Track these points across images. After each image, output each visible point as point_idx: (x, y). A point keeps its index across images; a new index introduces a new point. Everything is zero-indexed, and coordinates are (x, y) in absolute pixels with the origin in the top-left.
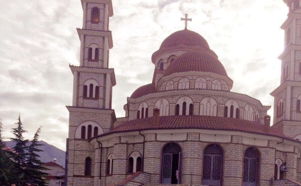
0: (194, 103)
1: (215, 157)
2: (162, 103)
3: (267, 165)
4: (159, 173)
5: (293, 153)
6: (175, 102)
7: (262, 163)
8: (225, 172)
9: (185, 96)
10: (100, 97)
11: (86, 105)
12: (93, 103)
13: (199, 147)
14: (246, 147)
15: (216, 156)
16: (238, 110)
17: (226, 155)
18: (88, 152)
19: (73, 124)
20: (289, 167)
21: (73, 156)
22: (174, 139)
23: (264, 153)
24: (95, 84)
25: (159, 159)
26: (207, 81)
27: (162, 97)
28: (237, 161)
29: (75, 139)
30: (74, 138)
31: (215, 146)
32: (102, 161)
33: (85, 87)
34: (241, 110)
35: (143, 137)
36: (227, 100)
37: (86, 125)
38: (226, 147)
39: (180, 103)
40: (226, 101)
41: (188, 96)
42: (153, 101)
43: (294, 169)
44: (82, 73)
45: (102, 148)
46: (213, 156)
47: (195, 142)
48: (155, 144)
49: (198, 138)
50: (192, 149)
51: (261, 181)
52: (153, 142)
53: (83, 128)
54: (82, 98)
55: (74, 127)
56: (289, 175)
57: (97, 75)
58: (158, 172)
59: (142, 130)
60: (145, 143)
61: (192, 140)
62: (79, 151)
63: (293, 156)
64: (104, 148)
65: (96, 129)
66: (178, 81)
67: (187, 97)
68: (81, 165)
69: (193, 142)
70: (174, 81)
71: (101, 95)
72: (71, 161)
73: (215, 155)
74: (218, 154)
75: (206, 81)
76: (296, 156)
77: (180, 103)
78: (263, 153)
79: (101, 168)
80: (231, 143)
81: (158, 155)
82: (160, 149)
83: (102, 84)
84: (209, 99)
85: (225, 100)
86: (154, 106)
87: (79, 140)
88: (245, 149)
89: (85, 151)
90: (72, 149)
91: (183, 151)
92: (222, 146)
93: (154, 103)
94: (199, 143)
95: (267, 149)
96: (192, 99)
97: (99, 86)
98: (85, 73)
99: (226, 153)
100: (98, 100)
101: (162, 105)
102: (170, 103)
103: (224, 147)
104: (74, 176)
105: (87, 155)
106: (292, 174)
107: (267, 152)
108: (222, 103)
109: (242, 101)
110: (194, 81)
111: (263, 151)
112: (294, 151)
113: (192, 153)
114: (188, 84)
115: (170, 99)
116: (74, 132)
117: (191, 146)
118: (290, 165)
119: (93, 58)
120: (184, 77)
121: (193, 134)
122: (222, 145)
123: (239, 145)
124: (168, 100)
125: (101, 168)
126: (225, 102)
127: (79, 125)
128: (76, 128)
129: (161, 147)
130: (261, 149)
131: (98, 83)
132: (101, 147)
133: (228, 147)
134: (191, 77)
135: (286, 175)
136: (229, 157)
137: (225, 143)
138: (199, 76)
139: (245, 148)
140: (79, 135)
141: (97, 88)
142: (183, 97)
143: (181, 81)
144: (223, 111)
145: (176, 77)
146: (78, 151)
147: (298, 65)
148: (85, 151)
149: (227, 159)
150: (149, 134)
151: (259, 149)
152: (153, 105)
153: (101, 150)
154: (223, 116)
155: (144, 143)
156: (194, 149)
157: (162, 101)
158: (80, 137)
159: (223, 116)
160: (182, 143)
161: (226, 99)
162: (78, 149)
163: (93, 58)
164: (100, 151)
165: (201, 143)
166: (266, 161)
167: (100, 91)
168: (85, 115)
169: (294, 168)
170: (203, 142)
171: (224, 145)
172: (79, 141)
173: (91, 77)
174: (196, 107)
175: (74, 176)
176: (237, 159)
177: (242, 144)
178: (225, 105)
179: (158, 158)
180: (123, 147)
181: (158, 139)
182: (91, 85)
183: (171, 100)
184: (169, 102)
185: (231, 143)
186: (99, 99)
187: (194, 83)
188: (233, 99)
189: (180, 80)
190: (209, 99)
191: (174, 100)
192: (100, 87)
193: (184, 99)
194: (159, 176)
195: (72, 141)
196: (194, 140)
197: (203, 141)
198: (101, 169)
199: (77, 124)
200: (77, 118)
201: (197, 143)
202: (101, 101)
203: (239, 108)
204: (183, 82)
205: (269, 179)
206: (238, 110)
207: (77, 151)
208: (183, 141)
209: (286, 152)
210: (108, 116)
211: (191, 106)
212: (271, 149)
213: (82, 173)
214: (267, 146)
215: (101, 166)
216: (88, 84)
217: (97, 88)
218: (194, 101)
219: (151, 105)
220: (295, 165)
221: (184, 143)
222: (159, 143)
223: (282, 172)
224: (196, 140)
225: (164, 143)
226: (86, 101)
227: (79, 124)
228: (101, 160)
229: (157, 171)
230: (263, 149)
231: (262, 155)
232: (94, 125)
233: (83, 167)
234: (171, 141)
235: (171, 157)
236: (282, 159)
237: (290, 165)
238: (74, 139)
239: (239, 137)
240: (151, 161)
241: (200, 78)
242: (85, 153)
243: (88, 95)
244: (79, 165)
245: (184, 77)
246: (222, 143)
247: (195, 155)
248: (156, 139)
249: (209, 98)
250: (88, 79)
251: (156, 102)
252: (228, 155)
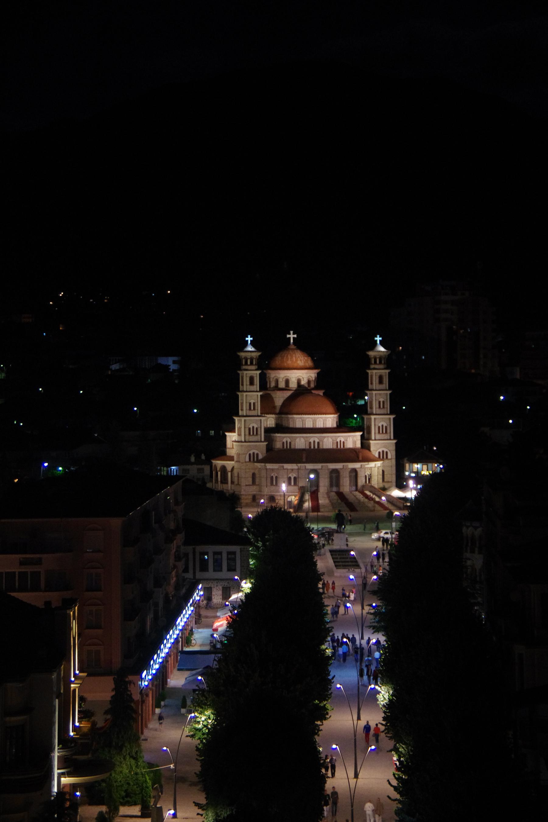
11: (250, 440)
16: (344, 442)
24: (256, 426)
33: (249, 429)
34: (345, 442)
37: (251, 452)
45: (267, 469)
53: (250, 455)
64: (268, 469)
65: (257, 454)
71: (259, 433)
87: (247, 462)
104: (246, 485)
105: (253, 471)
114: (312, 423)
119: (252, 408)
128: (245, 455)
140: (247, 459)
141: (257, 429)
144: (336, 444)
155: (298, 469)
158: (248, 461)
163: (252, 408)
174: (321, 443)
175: (246, 485)
182: (253, 427)
206: (344, 442)
211: (318, 443)
213: (251, 483)
216: (251, 427)
217: (257, 429)
223: (369, 479)
226: (250, 437)
232: (256, 452)
233: (251, 479)
243: (252, 433)
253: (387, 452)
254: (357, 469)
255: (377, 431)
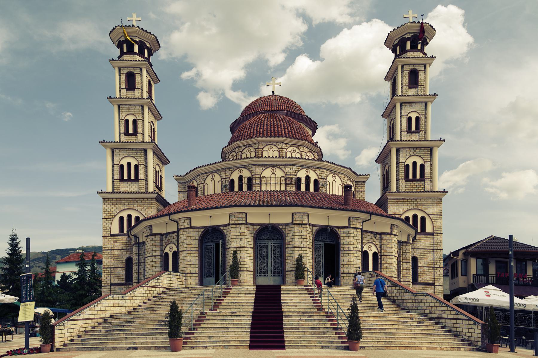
0: (252, 175)
1: (273, 243)
2: (213, 179)
3: (350, 252)
4: (197, 272)
5: (391, 234)
6: (229, 177)
7: (342, 249)
8: (287, 264)
9: (242, 167)
10: (140, 178)
11: (123, 189)
12: (131, 187)
13: (246, 231)
14: (317, 228)
15: (274, 242)
17: (286, 241)
18: (128, 250)
19: (108, 215)
20: (386, 254)
21: (110, 258)
22: (215, 222)
23: (344, 235)
24: (134, 163)
25: (197, 252)
26: (279, 148)
27: (213, 172)
28: (301, 248)
29: (112, 235)
30: (110, 234)
31: (270, 229)
32: (140, 262)
33: (122, 167)
35: (177, 223)
36: (299, 169)
37: (125, 214)
38: (287, 230)
39: (235, 176)
40: (299, 171)
41: (244, 167)
42: (203, 178)
43: (393, 257)
44: (116, 149)
46: (269, 243)
47: (240, 226)
48: (190, 232)
49: (244, 219)
50: (236, 234)
51: (342, 275)
52: (187, 230)
53: (122, 219)
54: (119, 180)
55: (110, 219)
56: (386, 265)
57: (135, 152)
58: (196, 269)
59: (172, 214)
60: (179, 232)
61: (236, 222)
62: (117, 250)
63: (391, 238)
66: (241, 152)
67: (244, 169)
68: (120, 269)
69: (238, 226)
70: (236, 152)
71: (142, 175)
72: (107, 264)
73: (273, 242)
74: (277, 240)
75: (278, 149)
76: (395, 239)
77: (235, 176)
78: (342, 235)
79: (138, 270)
80: (292, 223)
81: (195, 246)
82: (197, 238)
83: (141, 161)
84: (273, 170)
85: (297, 169)
86: (204, 183)
88: (314, 231)
89: (125, 249)
90: (107, 249)
91: (227, 239)
92: (281, 229)
93: (204, 180)
94: (246, 226)
95: (348, 229)
96: (250, 171)
97: (138, 164)
98: (120, 150)
99: (287, 238)
100: (138, 181)
101: (213, 181)
102: (223, 177)
103: (283, 230)
106: (391, 265)
107: (347, 234)
108: (292, 174)
109: (322, 170)
110: (261, 149)
111: (342, 233)
112: (392, 231)
113: (237, 240)
115: (222, 173)
116: (110, 226)
117: (235, 231)
118: (388, 251)
120: (249, 146)
121: (236, 214)
122: (281, 227)
123: (303, 226)
124: (220, 175)
125: (138, 270)
126: (296, 172)
127: (115, 216)
128: (112, 219)
129: (199, 235)
130: (340, 230)
131: (138, 161)
132: (137, 242)
133: (289, 229)
134: (257, 145)
135: (383, 265)
136: (291, 243)
137: (285, 225)
138: (268, 144)
139: (315, 229)
140: (115, 229)
141: (137, 167)
142: (238, 170)
143: (245, 151)
145: (238, 147)
146: (116, 251)
147: (406, 120)
148: (125, 249)
149: (289, 246)
150: (182, 219)
151: (337, 229)
152: (203, 182)
153: (139, 247)
154: (295, 190)
156: (239, 234)
157: (213, 177)
159: (295, 190)
160: (225, 228)
161: (298, 167)
162: (116, 248)
164: (137, 248)
165: (250, 226)
166: (347, 246)
167: (140, 170)
168: (123, 202)
169: (392, 256)
170: (254, 225)
171: (284, 227)
172: (116, 237)
173: (128, 153)
176: (302, 246)
177: (309, 224)
178: (296, 175)
179: (195, 251)
180: (156, 239)
181: (192, 225)
183: (223, 174)
184: (221, 177)
185: (292, 223)
186: (140, 181)
187: (261, 151)
188: (307, 168)
189: (243, 150)
190: (273, 170)
191: (226, 174)
192: (140, 166)
193: (240, 171)
194: (197, 275)
195: (108, 238)
196: (239, 222)
197: (253, 224)
198: (138, 272)
199: (113, 214)
200: (113, 206)
201: (243, 226)
202: (142, 183)
203: (317, 178)
204: (248, 152)
205: (352, 272)
207: (114, 251)
208: (226, 225)
209: (380, 234)
210: (151, 201)
212: (353, 230)
214: (347, 225)
215: (139, 268)
218: (253, 174)
219: (201, 183)
220: (393, 251)
221: (227, 227)
222: (195, 230)
224: (242, 222)
225: (202, 230)
226: (124, 184)
227: (115, 214)
228: (139, 260)
229: (195, 269)
230: (342, 230)
231: (342, 238)
234: (210, 226)
235: (213, 247)
236: (374, 243)
237: (388, 251)
238: (109, 235)
239: (302, 214)
240: (185, 255)
241: (270, 146)
242: (125, 253)
244: (118, 269)
245: (249, 147)
246: (281, 225)
247: (241, 242)
248: (191, 225)
249: (274, 168)
250: (125, 157)
251: (206, 178)
252: (289, 240)
253: (423, 219)
254: (339, 231)
255: (402, 175)
